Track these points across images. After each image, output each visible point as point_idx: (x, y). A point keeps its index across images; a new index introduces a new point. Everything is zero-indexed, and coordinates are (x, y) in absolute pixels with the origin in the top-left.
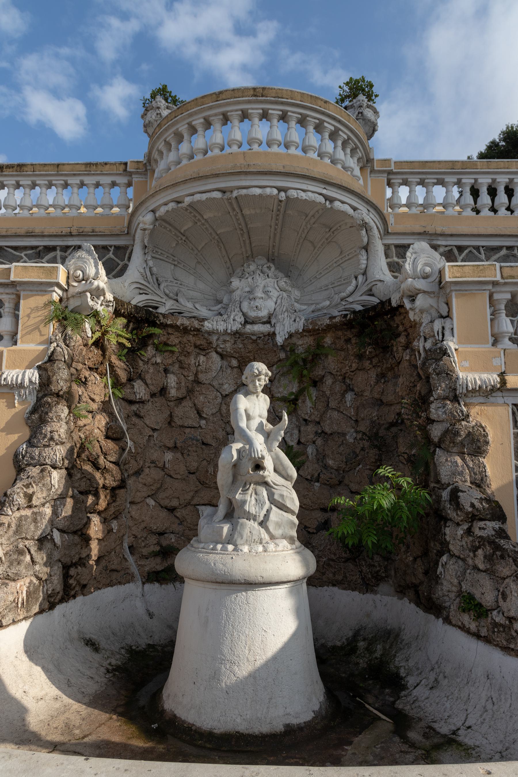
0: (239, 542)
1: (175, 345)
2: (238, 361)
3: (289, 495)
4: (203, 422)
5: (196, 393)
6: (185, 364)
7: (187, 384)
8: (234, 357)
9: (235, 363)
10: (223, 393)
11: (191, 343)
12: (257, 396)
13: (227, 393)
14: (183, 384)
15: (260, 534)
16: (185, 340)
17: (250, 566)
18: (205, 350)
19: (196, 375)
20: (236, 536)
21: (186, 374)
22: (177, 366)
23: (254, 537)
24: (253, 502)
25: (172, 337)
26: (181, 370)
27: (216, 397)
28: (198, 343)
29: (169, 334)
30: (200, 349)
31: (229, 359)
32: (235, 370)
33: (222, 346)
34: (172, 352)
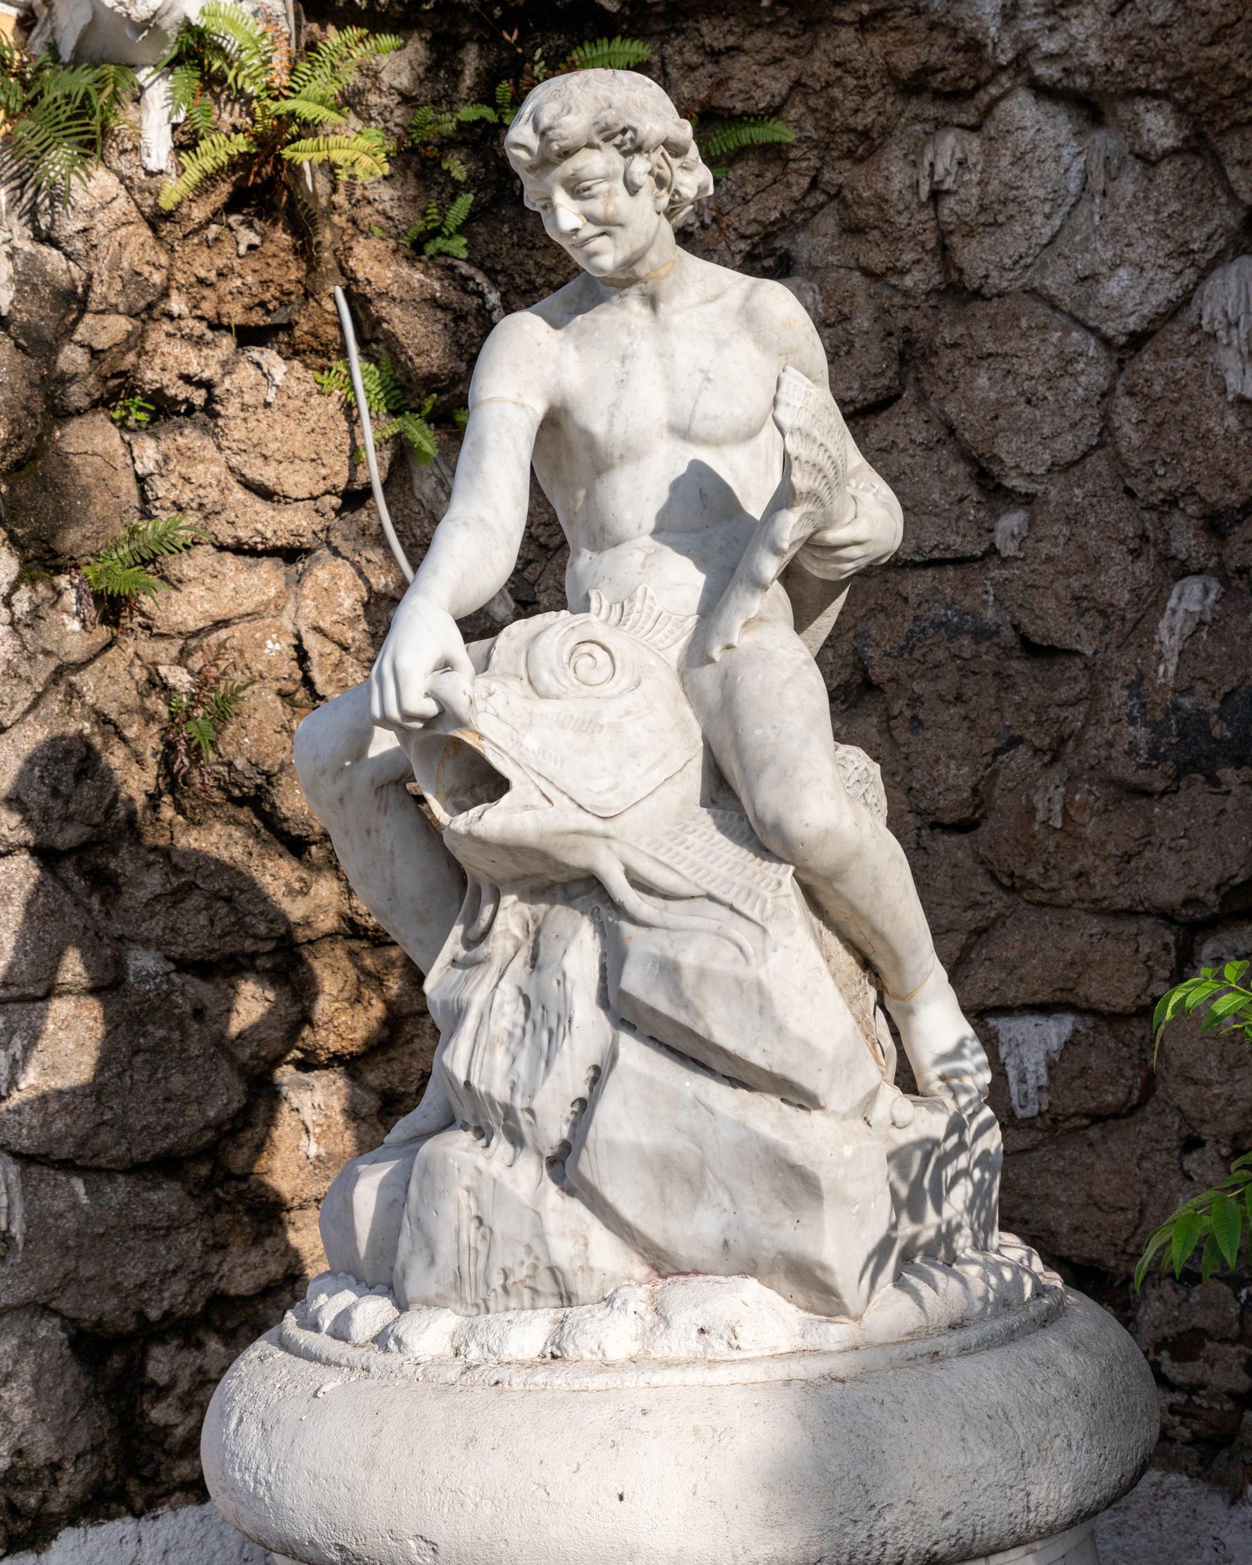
0: (417, 1283)
1: (775, 112)
2: (1180, 108)
3: (724, 961)
4: (1012, 521)
5: (947, 357)
6: (861, 203)
7: (902, 319)
8: (1147, 93)
9: (1159, 126)
10: (1110, 329)
11: (853, 72)
12: (652, 301)
13: (1133, 323)
14: (863, 321)
15: (541, 1236)
16: (819, 65)
17: (371, 1463)
18: (970, 94)
19: (944, 250)
20: (404, 1243)
21: (877, 259)
22: (828, 223)
23: (502, 1258)
24: (508, 1013)
25: (741, 70)
26: (854, 244)
27: (1067, 361)
28: (908, 60)
29: (714, 55)
30: (938, 95)
31: (1123, 112)
32: (1166, 171)
33: (1050, 45)
34: (774, 153)
